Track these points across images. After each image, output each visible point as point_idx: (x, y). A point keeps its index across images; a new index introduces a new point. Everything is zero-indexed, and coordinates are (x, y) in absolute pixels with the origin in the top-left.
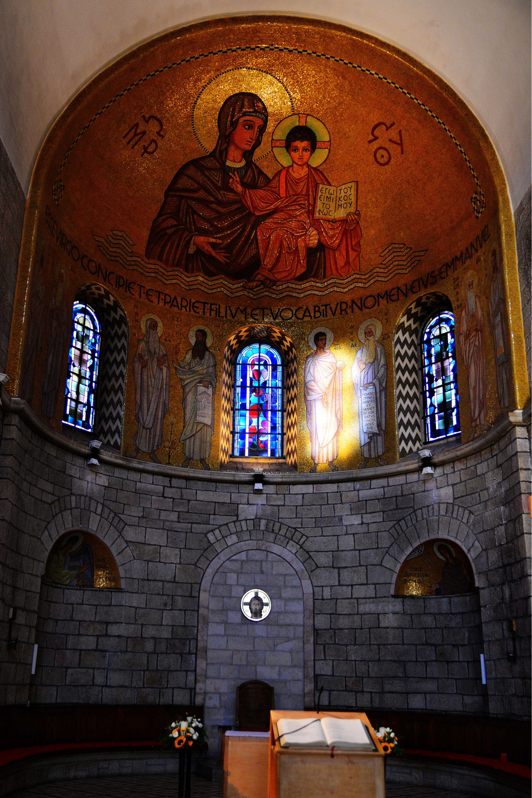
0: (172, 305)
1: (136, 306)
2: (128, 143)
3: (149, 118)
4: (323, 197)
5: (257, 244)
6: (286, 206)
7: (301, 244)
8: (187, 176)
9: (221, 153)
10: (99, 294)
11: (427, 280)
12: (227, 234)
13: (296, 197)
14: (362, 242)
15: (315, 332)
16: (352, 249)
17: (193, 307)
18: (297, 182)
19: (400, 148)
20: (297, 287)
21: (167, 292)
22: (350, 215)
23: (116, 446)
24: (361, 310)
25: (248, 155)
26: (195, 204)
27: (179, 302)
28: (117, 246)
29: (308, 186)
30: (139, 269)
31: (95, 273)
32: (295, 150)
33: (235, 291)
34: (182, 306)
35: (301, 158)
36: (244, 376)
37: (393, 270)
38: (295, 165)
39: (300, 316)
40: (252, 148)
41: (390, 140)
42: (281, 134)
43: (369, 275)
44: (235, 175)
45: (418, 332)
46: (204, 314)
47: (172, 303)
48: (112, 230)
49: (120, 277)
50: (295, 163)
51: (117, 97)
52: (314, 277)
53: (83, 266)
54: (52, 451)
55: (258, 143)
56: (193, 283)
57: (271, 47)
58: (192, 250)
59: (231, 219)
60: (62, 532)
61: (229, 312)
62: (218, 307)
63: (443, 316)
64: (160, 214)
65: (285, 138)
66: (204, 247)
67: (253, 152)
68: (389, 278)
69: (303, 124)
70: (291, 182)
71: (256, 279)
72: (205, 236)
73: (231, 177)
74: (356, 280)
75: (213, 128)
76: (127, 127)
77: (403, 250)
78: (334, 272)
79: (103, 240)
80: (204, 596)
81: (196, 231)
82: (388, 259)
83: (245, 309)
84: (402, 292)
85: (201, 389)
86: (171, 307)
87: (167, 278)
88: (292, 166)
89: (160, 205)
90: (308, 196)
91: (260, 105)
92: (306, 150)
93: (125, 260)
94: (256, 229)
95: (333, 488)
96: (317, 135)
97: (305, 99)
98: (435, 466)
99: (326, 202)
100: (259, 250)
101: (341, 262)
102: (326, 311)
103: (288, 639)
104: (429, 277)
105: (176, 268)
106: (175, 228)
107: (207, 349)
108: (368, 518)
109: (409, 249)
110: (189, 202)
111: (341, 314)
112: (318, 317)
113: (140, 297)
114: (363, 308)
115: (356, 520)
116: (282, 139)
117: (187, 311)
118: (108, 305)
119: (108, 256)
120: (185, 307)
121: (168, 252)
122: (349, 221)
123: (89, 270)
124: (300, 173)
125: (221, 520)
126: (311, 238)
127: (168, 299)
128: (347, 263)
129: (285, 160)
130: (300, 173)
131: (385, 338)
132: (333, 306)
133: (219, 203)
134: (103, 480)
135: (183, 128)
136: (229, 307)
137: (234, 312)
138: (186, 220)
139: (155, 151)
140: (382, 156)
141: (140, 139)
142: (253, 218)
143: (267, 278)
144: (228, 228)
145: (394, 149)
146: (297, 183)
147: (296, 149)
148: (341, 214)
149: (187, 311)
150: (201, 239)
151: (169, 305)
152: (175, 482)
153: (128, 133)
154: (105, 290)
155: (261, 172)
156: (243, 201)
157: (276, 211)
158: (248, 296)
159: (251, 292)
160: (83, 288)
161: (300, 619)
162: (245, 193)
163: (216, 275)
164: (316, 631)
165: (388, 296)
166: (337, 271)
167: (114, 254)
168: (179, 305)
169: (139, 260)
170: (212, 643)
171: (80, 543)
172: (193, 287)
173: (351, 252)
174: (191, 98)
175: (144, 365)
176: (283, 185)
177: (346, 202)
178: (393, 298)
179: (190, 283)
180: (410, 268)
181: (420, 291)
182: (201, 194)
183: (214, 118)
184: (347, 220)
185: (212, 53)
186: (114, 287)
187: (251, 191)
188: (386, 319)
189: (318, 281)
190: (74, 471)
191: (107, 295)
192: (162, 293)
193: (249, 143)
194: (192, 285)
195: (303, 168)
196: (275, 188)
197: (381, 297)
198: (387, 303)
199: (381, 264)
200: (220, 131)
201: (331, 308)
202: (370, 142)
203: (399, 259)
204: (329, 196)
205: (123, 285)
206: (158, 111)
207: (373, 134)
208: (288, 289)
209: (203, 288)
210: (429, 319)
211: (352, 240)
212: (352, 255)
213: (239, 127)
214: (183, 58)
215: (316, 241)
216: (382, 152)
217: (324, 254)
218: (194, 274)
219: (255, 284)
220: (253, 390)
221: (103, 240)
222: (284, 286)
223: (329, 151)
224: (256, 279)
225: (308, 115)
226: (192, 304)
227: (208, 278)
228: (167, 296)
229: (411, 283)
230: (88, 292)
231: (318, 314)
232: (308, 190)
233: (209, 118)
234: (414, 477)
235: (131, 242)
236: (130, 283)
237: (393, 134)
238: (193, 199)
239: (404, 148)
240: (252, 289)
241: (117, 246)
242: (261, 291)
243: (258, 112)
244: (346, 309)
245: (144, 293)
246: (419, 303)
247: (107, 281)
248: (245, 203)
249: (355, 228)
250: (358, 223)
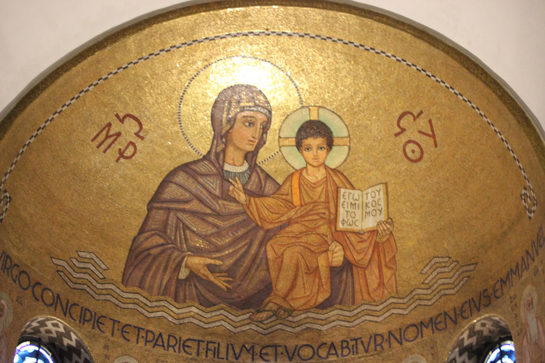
0: (155, 344)
1: (106, 347)
2: (98, 147)
3: (125, 117)
4: (346, 204)
5: (267, 264)
6: (301, 217)
7: (322, 262)
8: (175, 183)
9: (217, 155)
10: (57, 332)
11: (480, 300)
12: (229, 254)
13: (312, 206)
14: (397, 258)
16: (386, 266)
17: (184, 345)
18: (314, 186)
19: (432, 140)
20: (319, 316)
21: (150, 328)
22: (381, 224)
24: (401, 343)
26: (187, 217)
27: (166, 341)
28: (85, 271)
29: (327, 191)
30: (113, 300)
31: (51, 305)
32: (308, 149)
33: (238, 324)
34: (169, 346)
35: (316, 158)
37: (438, 290)
38: (309, 167)
40: (255, 149)
41: (420, 132)
42: (291, 131)
43: (409, 298)
44: (236, 182)
46: (198, 355)
48: (77, 252)
49: (86, 309)
50: (309, 164)
51: (80, 93)
52: (340, 304)
53: (34, 295)
55: (261, 143)
56: (184, 315)
57: (267, 32)
58: (183, 274)
59: (233, 234)
61: (231, 352)
62: (216, 345)
63: (505, 348)
64: (142, 231)
65: (294, 136)
66: (199, 270)
67: (258, 152)
68: (433, 301)
69: (314, 117)
71: (267, 308)
72: (200, 256)
73: (231, 183)
74: (392, 306)
75: (206, 126)
76: (96, 128)
77: (448, 265)
78: (366, 296)
79: (65, 264)
81: (189, 250)
82: (430, 278)
83: (253, 347)
84: (451, 318)
86: (154, 347)
87: (150, 310)
88: (306, 168)
89: (141, 220)
90: (327, 202)
91: (261, 98)
92: (321, 148)
93: (94, 289)
94: (266, 246)
96: (332, 129)
97: (315, 89)
99: (351, 210)
100: (269, 272)
102: (357, 348)
104: (482, 297)
105: (163, 298)
106: (161, 248)
109: (456, 263)
110: (180, 215)
111: (376, 350)
112: (347, 355)
113: (112, 335)
114: (404, 341)
116: (291, 136)
117: (175, 351)
118: (70, 347)
119: (70, 284)
120: (173, 347)
121: (152, 277)
122: (380, 232)
123: (43, 301)
126: (335, 255)
127: (150, 336)
128: (381, 284)
132: (365, 340)
133: (218, 215)
135: (168, 128)
136: (232, 345)
137: (237, 351)
138: (176, 238)
139: (133, 155)
140: (413, 151)
141: (113, 142)
142: (261, 233)
143: (280, 307)
144: (230, 245)
145: (426, 142)
146: (313, 188)
148: (370, 223)
149: (175, 351)
150: (196, 261)
151: (152, 344)
153: (98, 135)
154: (65, 328)
155: (268, 176)
156: (248, 212)
157: (289, 222)
158: (256, 331)
159: (261, 325)
160: (35, 324)
162: (250, 200)
163: (215, 305)
166: (369, 294)
167: (79, 281)
168: (166, 345)
169: (113, 287)
172: (186, 321)
173: (385, 270)
174: (176, 92)
177: (375, 208)
178: (439, 326)
179: (181, 316)
180: (458, 288)
181: (471, 315)
182: (195, 205)
183: (206, 115)
184: (377, 231)
185: (196, 41)
186: (78, 322)
187: (256, 199)
188: (432, 355)
189: (345, 308)
192: (143, 329)
193: (251, 143)
194: (183, 318)
195: (319, 170)
196: (287, 195)
197: (425, 326)
198: (433, 333)
199: (423, 283)
200: (214, 130)
201: (362, 342)
202: (397, 135)
203: (445, 277)
204: (353, 202)
205: (90, 320)
206: (136, 109)
207: (399, 126)
208: (308, 320)
209: (197, 322)
210: (488, 353)
211: (385, 254)
212: (387, 273)
213: (238, 125)
214: (162, 48)
215: (342, 259)
216: (411, 146)
217: (352, 275)
218: (186, 305)
219: (264, 315)
221: (65, 264)
222: (303, 316)
223: (349, 149)
224: (267, 308)
225: (320, 107)
226: (182, 342)
227: (203, 308)
228: (149, 334)
229: (460, 305)
230: (42, 329)
231: (346, 351)
232: (327, 196)
233: (200, 115)
235: (103, 266)
236: (99, 318)
237: (422, 123)
238: (184, 211)
239: (437, 139)
240: (261, 322)
241: (85, 271)
242: (273, 323)
243: (259, 106)
244: (382, 343)
245: (118, 330)
246: (472, 332)
247: (68, 315)
248: (250, 215)
249: (388, 240)
250: (391, 233)
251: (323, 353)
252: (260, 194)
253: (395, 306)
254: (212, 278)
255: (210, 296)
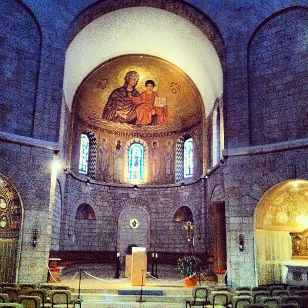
15: (153, 142)
23: (94, 178)
25: (134, 87)
36: (132, 154)
39: (149, 136)
45: (183, 144)
47: (110, 132)
54: (77, 181)
55: (137, 84)
60: (80, 204)
64: (107, 105)
70: (147, 95)
80: (119, 221)
85: (119, 159)
90: (152, 99)
95: (157, 190)
98: (185, 185)
101: (162, 121)
103: (142, 233)
107: (120, 147)
108: (166, 199)
115: (163, 200)
124: (149, 93)
125: (124, 199)
128: (163, 121)
129: (145, 89)
130: (149, 93)
131: (174, 145)
133: (125, 101)
134: (91, 188)
147: (148, 86)
148: (162, 106)
150: (118, 112)
152: (112, 188)
155: (138, 92)
157: (142, 103)
161: (146, 228)
164: (151, 231)
165: (175, 132)
170: (121, 234)
171: (83, 207)
175: (102, 153)
176: (144, 95)
182: (119, 98)
190: (82, 186)
191: (90, 132)
220: (135, 158)
234: (179, 188)
237: (177, 86)
246: (183, 136)
251: (149, 136)
252: (135, 96)
253: (167, 127)
254: (123, 116)
255: (122, 121)
